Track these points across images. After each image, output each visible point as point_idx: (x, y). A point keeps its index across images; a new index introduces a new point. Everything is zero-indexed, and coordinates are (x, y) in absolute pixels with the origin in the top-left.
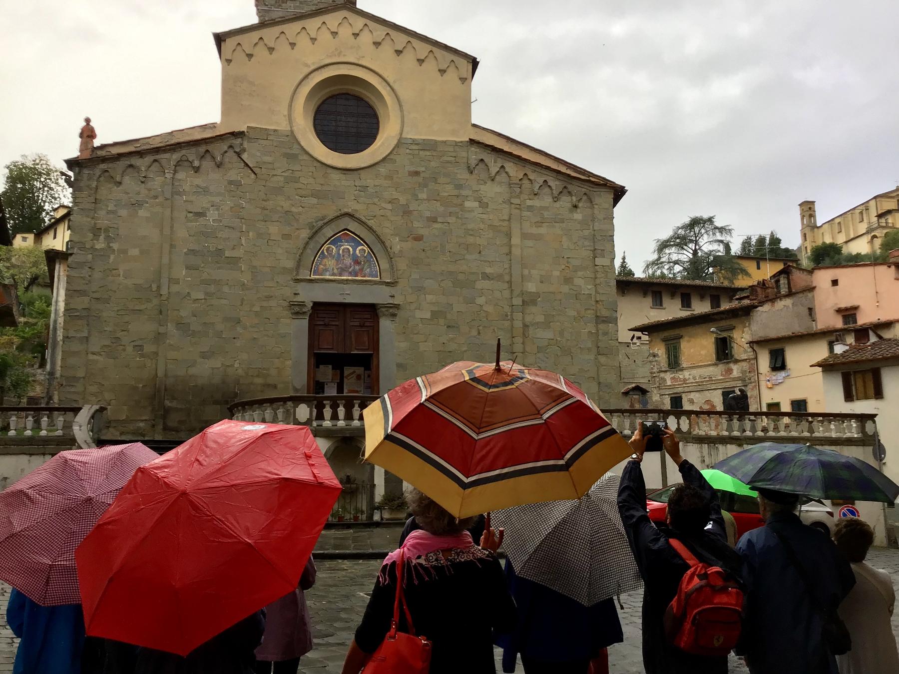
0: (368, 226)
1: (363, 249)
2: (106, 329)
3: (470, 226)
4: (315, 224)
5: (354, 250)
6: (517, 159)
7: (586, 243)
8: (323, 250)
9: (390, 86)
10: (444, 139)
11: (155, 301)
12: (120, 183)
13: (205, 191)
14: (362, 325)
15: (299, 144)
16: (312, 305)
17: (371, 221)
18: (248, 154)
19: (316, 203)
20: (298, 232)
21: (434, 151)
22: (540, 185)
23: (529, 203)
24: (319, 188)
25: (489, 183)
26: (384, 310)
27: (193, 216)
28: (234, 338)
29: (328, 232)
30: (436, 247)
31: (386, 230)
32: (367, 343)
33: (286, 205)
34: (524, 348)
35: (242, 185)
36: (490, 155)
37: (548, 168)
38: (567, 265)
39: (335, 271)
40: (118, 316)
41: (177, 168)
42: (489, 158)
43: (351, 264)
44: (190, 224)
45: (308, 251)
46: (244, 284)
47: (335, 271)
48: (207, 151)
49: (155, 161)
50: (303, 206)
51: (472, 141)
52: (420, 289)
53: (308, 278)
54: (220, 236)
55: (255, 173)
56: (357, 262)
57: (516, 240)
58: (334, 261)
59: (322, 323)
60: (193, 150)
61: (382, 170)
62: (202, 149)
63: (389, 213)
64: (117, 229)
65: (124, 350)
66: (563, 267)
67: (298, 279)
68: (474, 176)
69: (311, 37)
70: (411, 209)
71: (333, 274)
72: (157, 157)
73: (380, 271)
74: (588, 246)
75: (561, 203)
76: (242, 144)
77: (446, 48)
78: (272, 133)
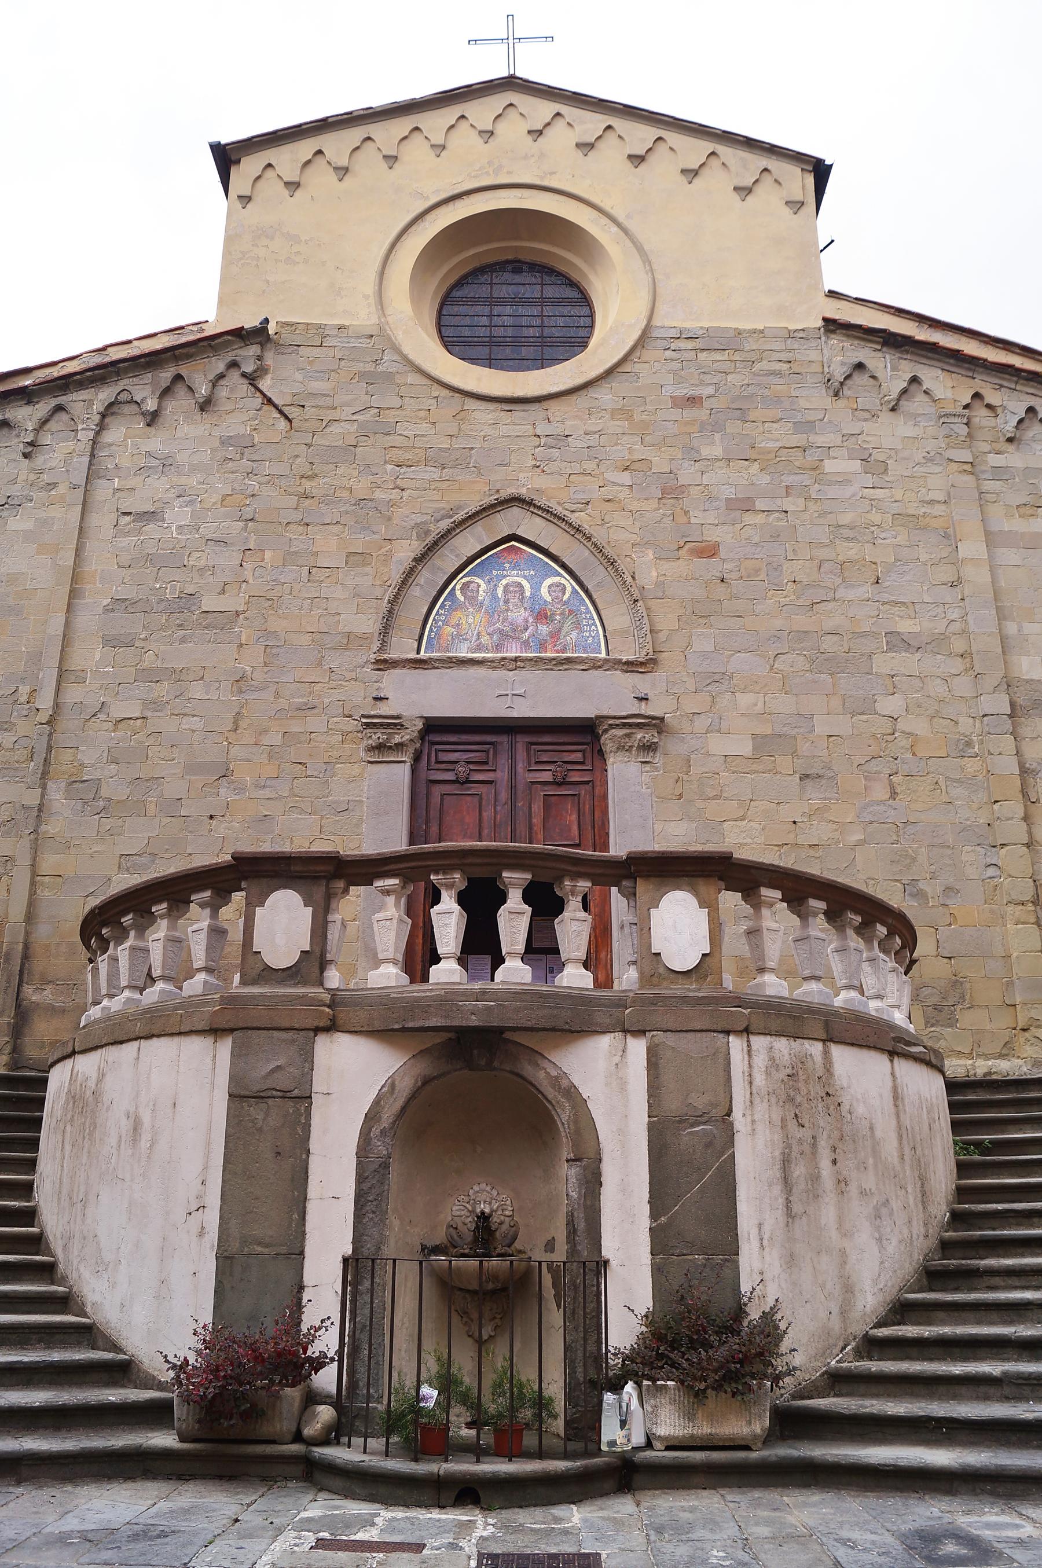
3: (846, 519)
4: (432, 527)
5: (536, 589)
6: (952, 361)
8: (454, 589)
9: (618, 224)
11: (23, 728)
13: (166, 464)
15: (398, 351)
16: (420, 725)
17: (577, 514)
18: (272, 379)
19: (436, 476)
22: (1017, 418)
23: (994, 460)
25: (886, 416)
27: (134, 521)
28: (211, 817)
29: (468, 543)
30: (757, 571)
32: (575, 828)
33: (361, 485)
34: (1030, 833)
36: (880, 354)
41: (107, 420)
42: (878, 360)
47: (485, 640)
48: (178, 378)
49: (60, 408)
50: (404, 486)
51: (832, 325)
53: (413, 655)
54: (191, 563)
55: (286, 417)
56: (542, 616)
57: (972, 548)
59: (450, 776)
60: (148, 377)
61: (605, 396)
62: (166, 375)
63: (624, 494)
67: (385, 661)
68: (841, 403)
69: (433, 142)
71: (479, 648)
72: (62, 400)
73: (605, 636)
76: (260, 358)
77: (750, 144)
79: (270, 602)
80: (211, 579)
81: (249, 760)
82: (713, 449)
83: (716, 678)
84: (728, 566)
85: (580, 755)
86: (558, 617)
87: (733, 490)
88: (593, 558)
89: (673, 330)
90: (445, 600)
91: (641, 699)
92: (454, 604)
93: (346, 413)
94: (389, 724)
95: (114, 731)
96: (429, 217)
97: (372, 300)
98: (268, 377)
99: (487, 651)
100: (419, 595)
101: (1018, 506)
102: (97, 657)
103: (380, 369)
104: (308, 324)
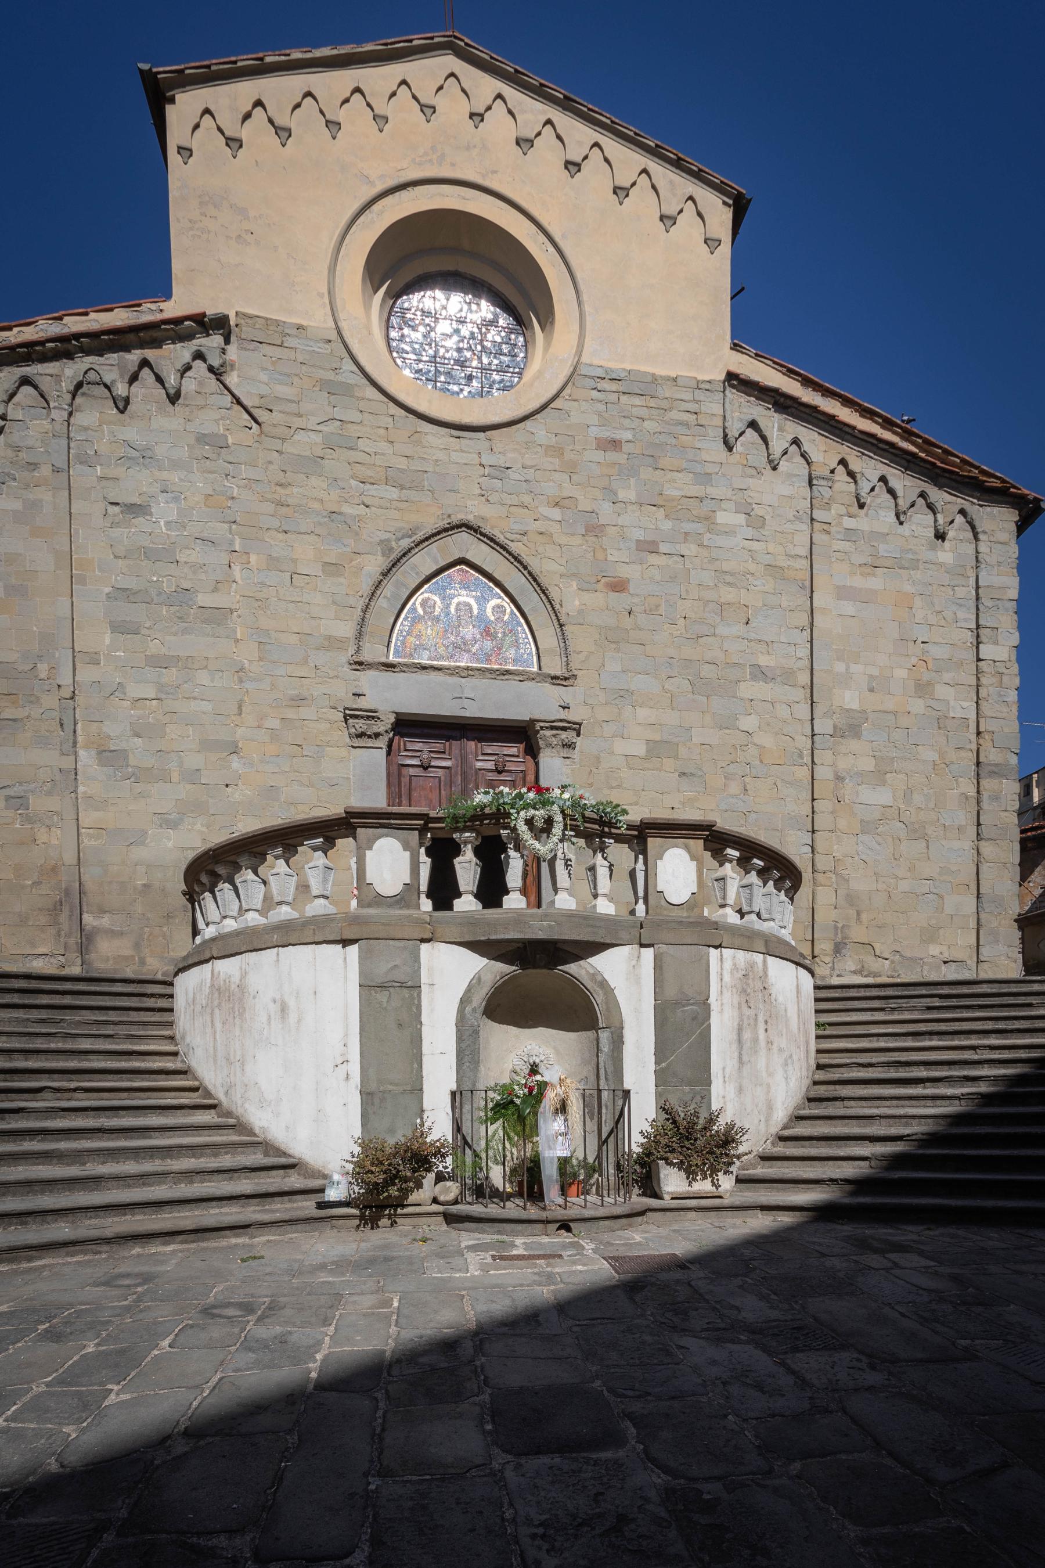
0: (510, 554)
1: (499, 606)
8: (414, 604)
13: (145, 457)
14: (500, 768)
16: (393, 720)
18: (239, 376)
19: (395, 496)
20: (359, 559)
24: (402, 463)
26: (548, 733)
30: (658, 606)
39: (441, 650)
44: (116, 532)
46: (242, 669)
50: (368, 503)
52: (623, 695)
53: (383, 660)
54: (185, 560)
56: (487, 633)
60: (113, 357)
62: (134, 356)
63: (555, 528)
67: (361, 663)
70: (601, 522)
78: (293, 332)
79: (260, 603)
80: (203, 577)
81: (253, 740)
82: (627, 493)
83: (623, 695)
84: (636, 600)
85: (515, 749)
87: (642, 532)
89: (599, 369)
90: (408, 612)
91: (564, 708)
92: (416, 620)
93: (312, 422)
94: (368, 717)
95: (132, 709)
98: (235, 374)
99: (442, 658)
100: (384, 603)
103: (340, 378)
104: (267, 319)
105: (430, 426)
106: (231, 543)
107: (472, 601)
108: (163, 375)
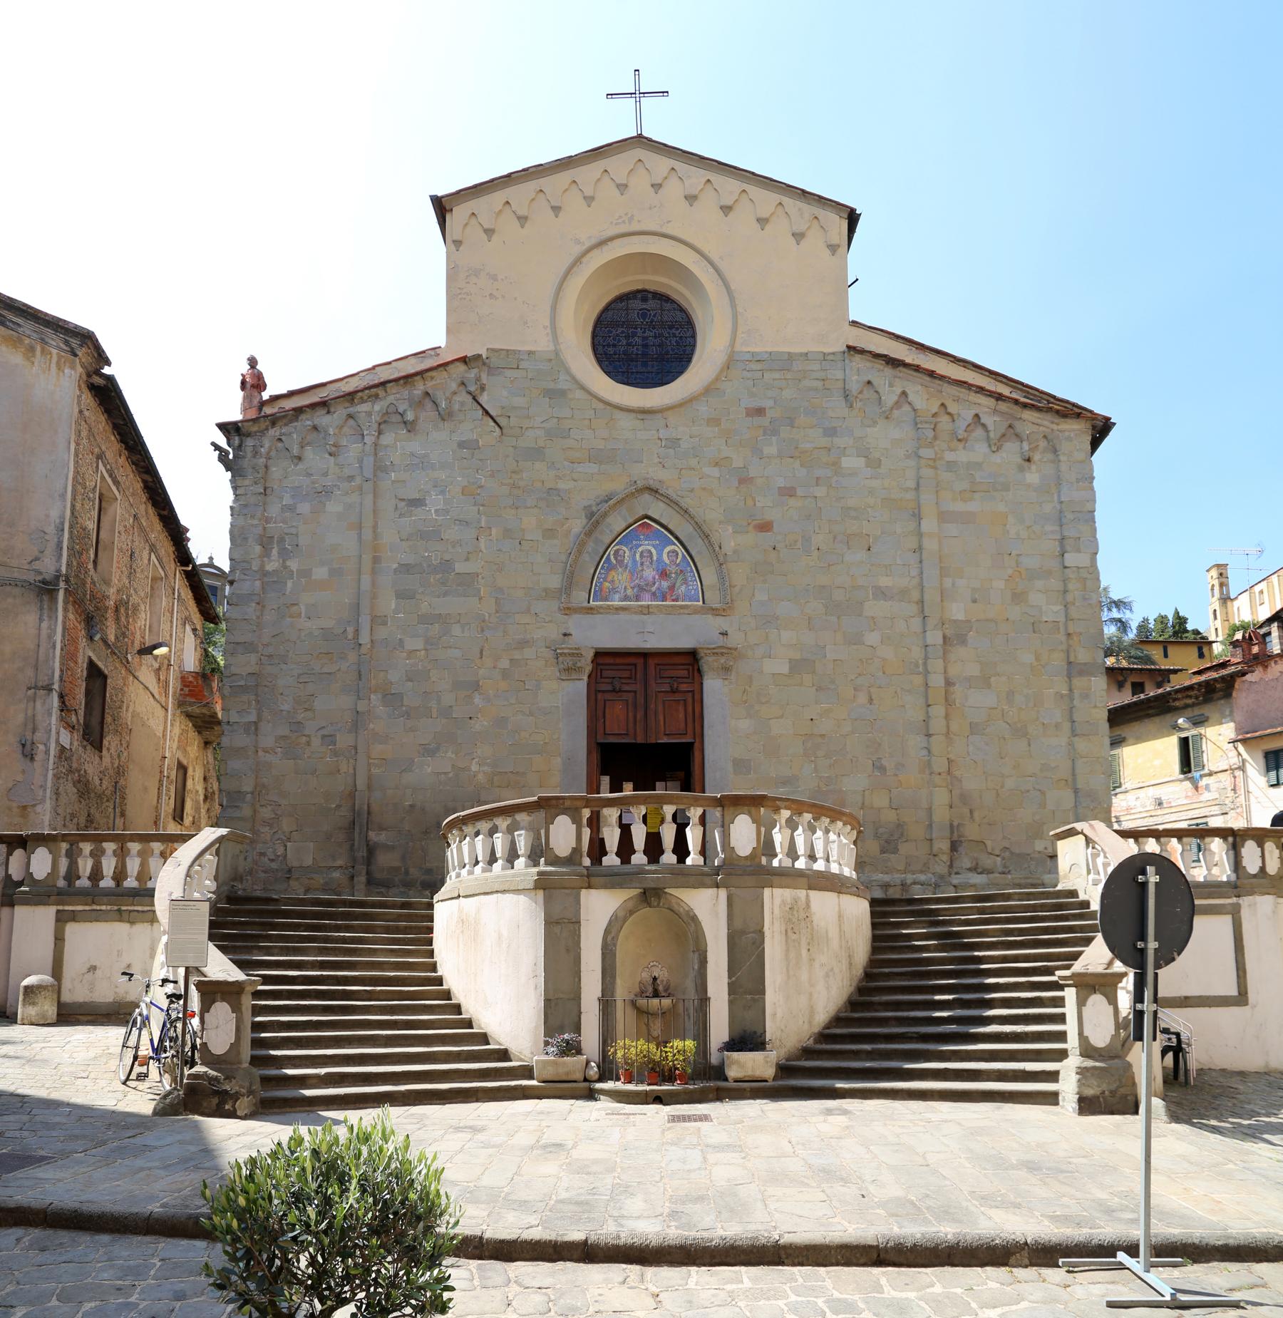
1: (674, 551)
2: (282, 708)
4: (594, 509)
5: (660, 554)
7: (1048, 528)
10: (804, 350)
12: (300, 458)
15: (568, 372)
18: (488, 395)
21: (788, 370)
23: (949, 456)
29: (617, 522)
30: (796, 541)
31: (710, 512)
35: (479, 448)
37: (981, 390)
38: (1016, 569)
40: (300, 685)
41: (382, 426)
42: (882, 377)
43: (654, 578)
45: (586, 557)
47: (629, 592)
49: (350, 416)
53: (585, 604)
54: (447, 537)
56: (664, 574)
57: (929, 525)
58: (626, 575)
61: (703, 409)
64: (297, 535)
65: (308, 743)
66: (1010, 572)
67: (568, 608)
71: (626, 598)
72: (352, 410)
73: (702, 589)
74: (1052, 532)
75: (1004, 455)
82: (771, 450)
86: (673, 575)
88: (695, 533)
92: (611, 568)
96: (585, 260)
97: (549, 330)
98: (485, 394)
101: (960, 492)
102: (393, 606)
104: (508, 351)
105: (622, 413)
106: (479, 521)
107: (653, 551)
108: (438, 401)
